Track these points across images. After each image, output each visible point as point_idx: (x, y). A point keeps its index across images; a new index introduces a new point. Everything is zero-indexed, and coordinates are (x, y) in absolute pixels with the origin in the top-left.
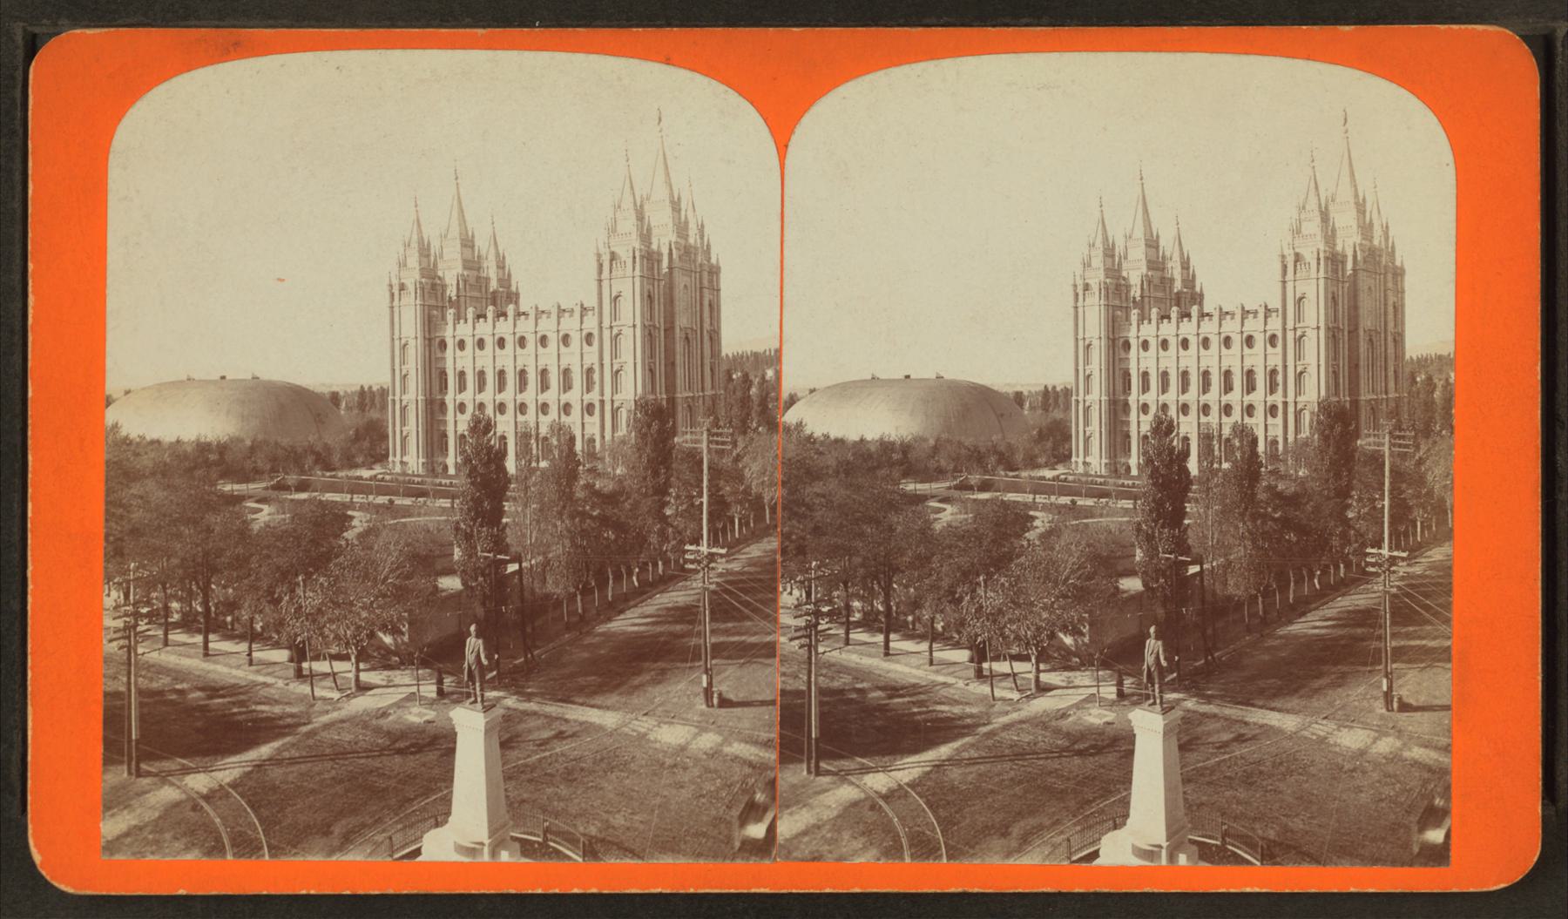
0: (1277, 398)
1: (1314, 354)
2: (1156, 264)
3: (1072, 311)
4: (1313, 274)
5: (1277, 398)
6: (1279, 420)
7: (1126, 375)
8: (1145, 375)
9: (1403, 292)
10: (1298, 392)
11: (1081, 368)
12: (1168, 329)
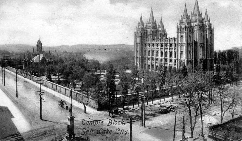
0: (176, 58)
1: (184, 48)
6: (176, 64)
7: (145, 52)
10: (181, 58)
11: (136, 50)
12: (154, 42)
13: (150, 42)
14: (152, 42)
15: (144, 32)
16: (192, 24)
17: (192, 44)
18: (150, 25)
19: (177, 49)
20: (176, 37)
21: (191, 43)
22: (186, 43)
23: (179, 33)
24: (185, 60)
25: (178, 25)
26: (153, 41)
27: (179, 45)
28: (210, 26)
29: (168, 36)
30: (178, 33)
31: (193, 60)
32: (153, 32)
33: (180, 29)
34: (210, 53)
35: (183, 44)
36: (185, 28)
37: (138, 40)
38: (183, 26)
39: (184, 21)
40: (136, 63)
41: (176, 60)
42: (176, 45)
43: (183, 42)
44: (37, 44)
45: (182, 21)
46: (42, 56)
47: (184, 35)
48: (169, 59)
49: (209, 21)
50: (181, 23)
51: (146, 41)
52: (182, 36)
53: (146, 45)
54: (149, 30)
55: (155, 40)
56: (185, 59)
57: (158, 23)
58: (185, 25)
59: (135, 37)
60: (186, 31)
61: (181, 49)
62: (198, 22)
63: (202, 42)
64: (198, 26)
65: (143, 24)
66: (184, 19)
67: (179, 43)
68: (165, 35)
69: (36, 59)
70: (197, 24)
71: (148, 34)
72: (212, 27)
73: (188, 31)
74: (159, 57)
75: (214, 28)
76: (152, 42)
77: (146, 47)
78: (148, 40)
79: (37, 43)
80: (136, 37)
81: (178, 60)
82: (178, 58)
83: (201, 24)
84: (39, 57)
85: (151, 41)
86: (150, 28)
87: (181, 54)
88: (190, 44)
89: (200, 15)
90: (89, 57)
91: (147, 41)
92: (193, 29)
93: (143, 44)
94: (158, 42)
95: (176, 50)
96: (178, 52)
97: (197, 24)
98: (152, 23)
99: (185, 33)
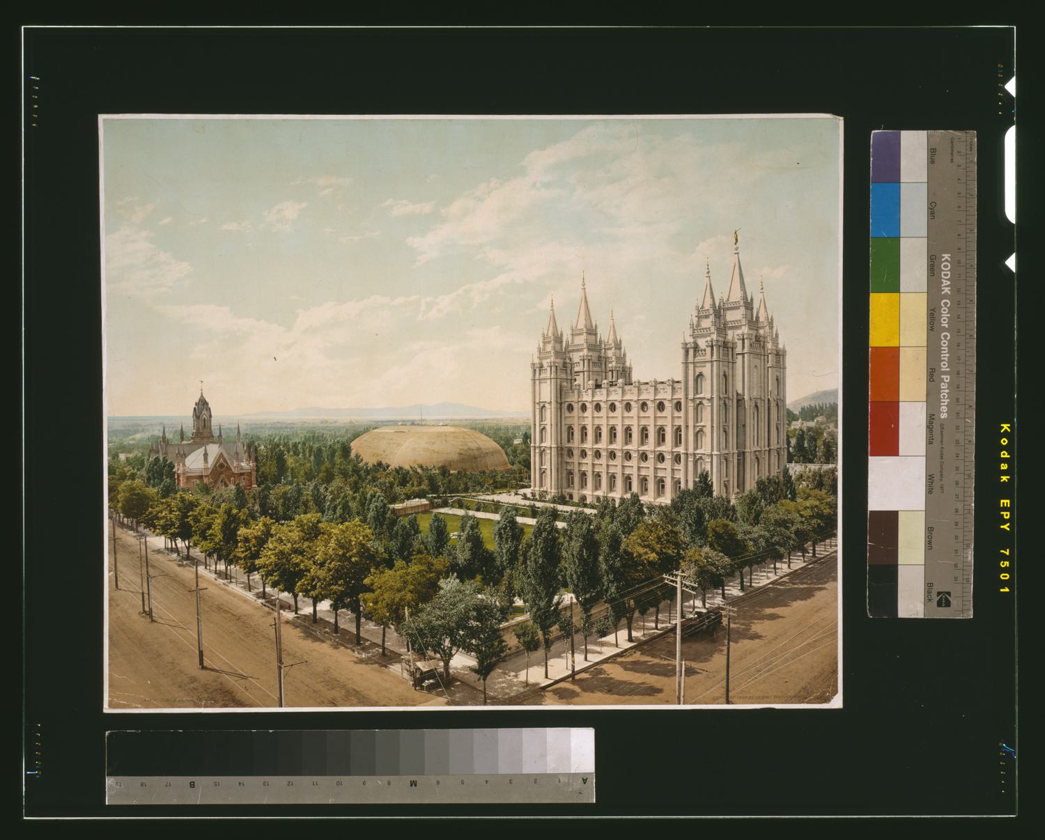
0: (681, 449)
2: (595, 347)
3: (530, 383)
4: (708, 357)
5: (681, 449)
6: (681, 467)
8: (584, 428)
9: (784, 368)
12: (601, 396)
13: (587, 397)
14: (593, 396)
15: (600, 357)
16: (730, 333)
17: (731, 402)
18: (581, 340)
19: (683, 419)
20: (679, 377)
21: (729, 398)
22: (715, 396)
23: (691, 366)
24: (712, 455)
25: (533, 361)
26: (598, 393)
27: (691, 404)
28: (621, 359)
29: (635, 378)
30: (686, 363)
31: (733, 454)
32: (591, 364)
33: (695, 351)
34: (777, 429)
35: (705, 402)
36: (712, 350)
37: (547, 392)
38: (702, 343)
39: (549, 347)
40: (540, 469)
41: (683, 457)
42: (678, 406)
43: (702, 396)
44: (195, 409)
45: (698, 325)
46: (214, 450)
47: (706, 370)
48: (672, 452)
49: (618, 346)
50: (696, 331)
51: (573, 392)
52: (701, 375)
53: (570, 408)
54: (576, 357)
55: (604, 391)
56: (712, 450)
57: (604, 334)
58: (709, 339)
59: (534, 380)
60: (715, 358)
61: (696, 420)
62: (585, 352)
63: (755, 394)
64: (746, 341)
65: (558, 339)
66: (707, 317)
67: (691, 396)
68: (625, 373)
69: (196, 462)
70: (712, 341)
71: (576, 369)
72: (628, 364)
73: (721, 356)
74: (650, 446)
75: (633, 366)
76: (593, 396)
77: (572, 415)
78: (579, 392)
79: (194, 406)
80: (537, 382)
81: (687, 454)
82: (687, 449)
83: (595, 355)
84: (206, 455)
85: (590, 392)
86: (581, 350)
87: (699, 433)
88: (727, 400)
89: (592, 331)
90: (366, 451)
91: (576, 392)
92: (571, 370)
93: (561, 404)
94: (616, 396)
95: (681, 422)
96: (687, 426)
97: (743, 335)
98: (587, 333)
99: (712, 366)
